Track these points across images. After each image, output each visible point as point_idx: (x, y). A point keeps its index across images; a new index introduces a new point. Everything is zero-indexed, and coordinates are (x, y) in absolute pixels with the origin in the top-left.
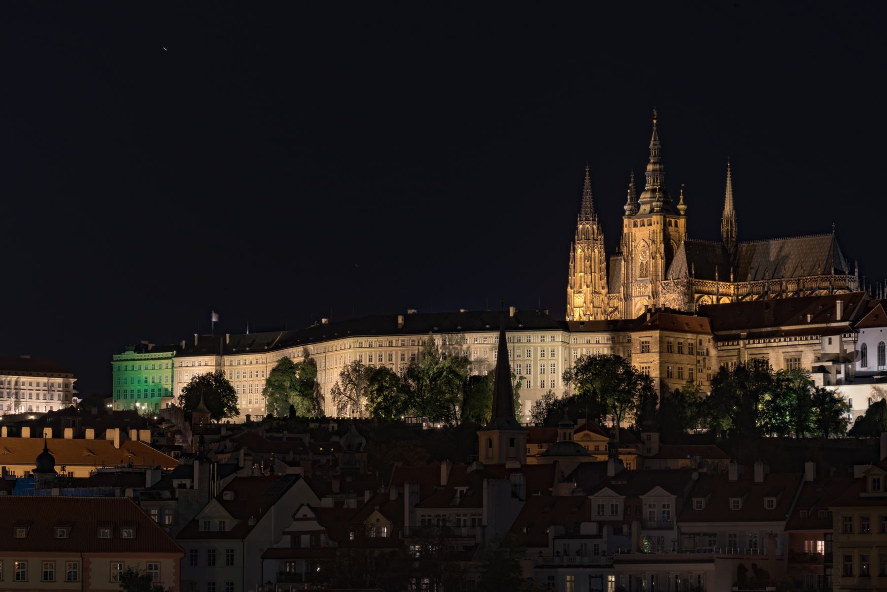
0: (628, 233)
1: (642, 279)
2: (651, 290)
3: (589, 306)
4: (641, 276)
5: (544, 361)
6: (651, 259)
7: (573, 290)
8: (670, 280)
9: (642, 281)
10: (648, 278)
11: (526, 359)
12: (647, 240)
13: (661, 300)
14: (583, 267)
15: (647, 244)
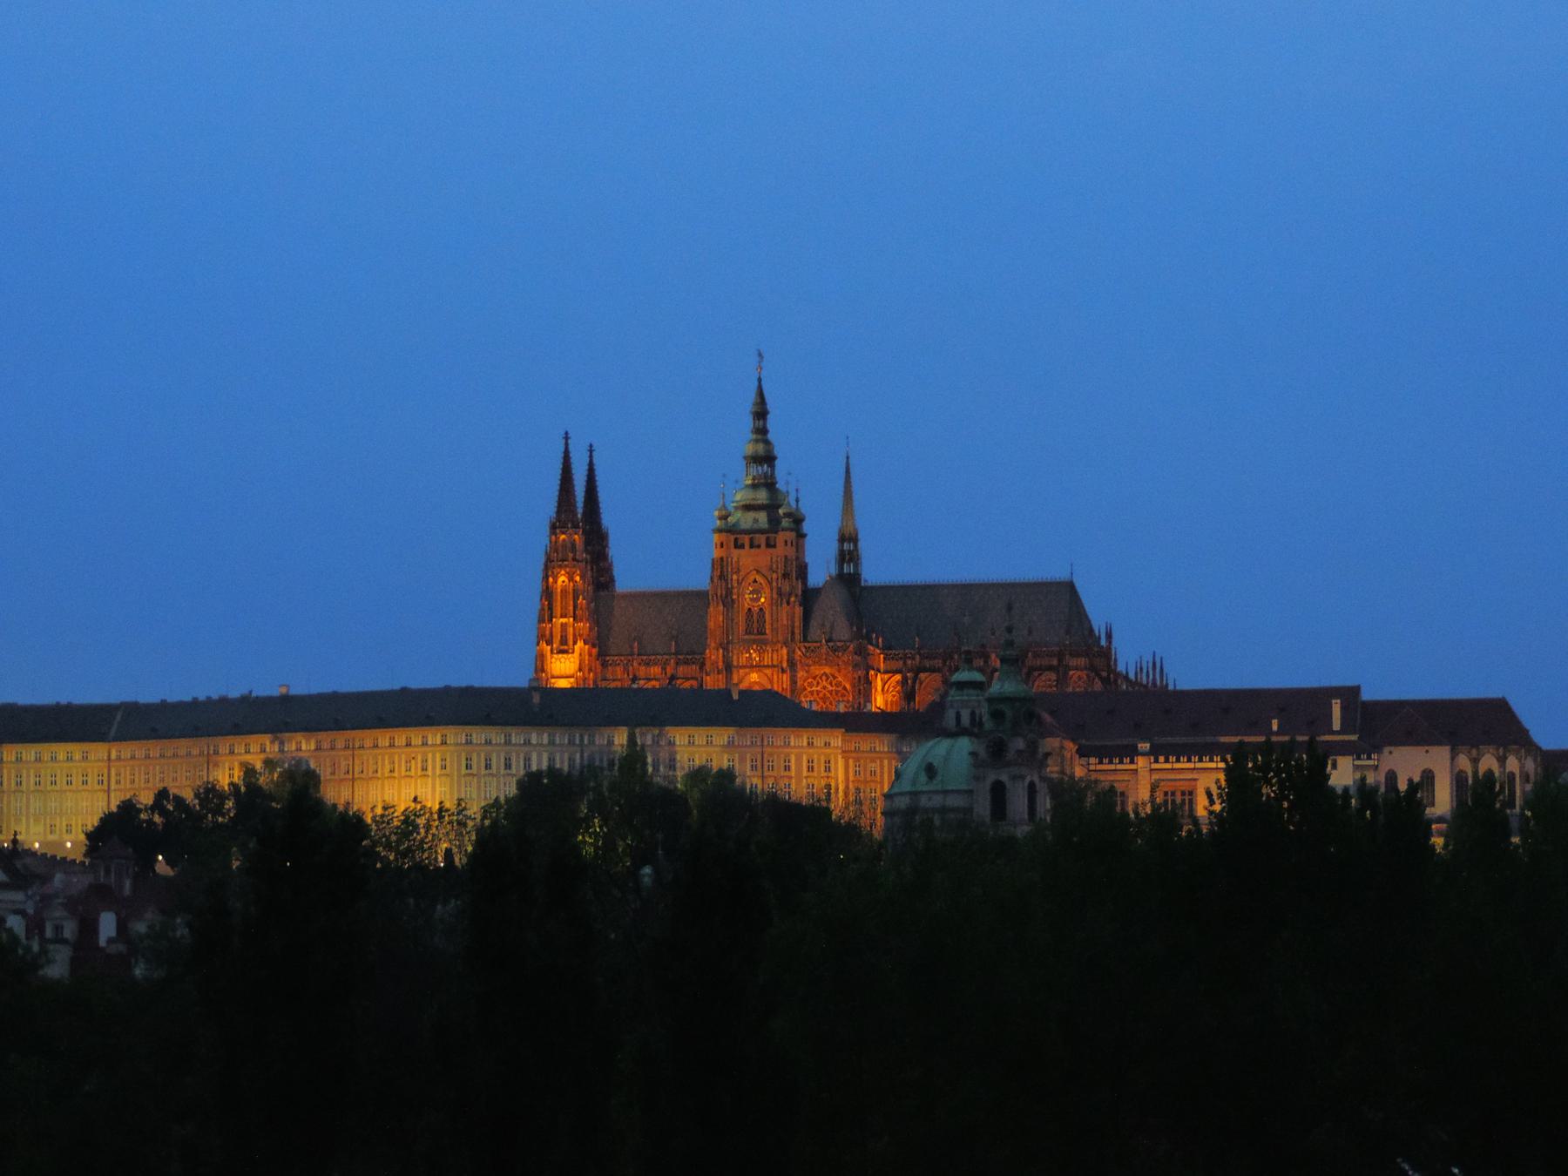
0: (727, 558)
1: (753, 637)
2: (785, 657)
3: (587, 676)
4: (747, 633)
5: (812, 780)
6: (785, 605)
7: (549, 648)
8: (821, 641)
9: (754, 642)
10: (767, 637)
11: (782, 774)
12: (764, 571)
13: (799, 675)
14: (571, 608)
15: (767, 579)
